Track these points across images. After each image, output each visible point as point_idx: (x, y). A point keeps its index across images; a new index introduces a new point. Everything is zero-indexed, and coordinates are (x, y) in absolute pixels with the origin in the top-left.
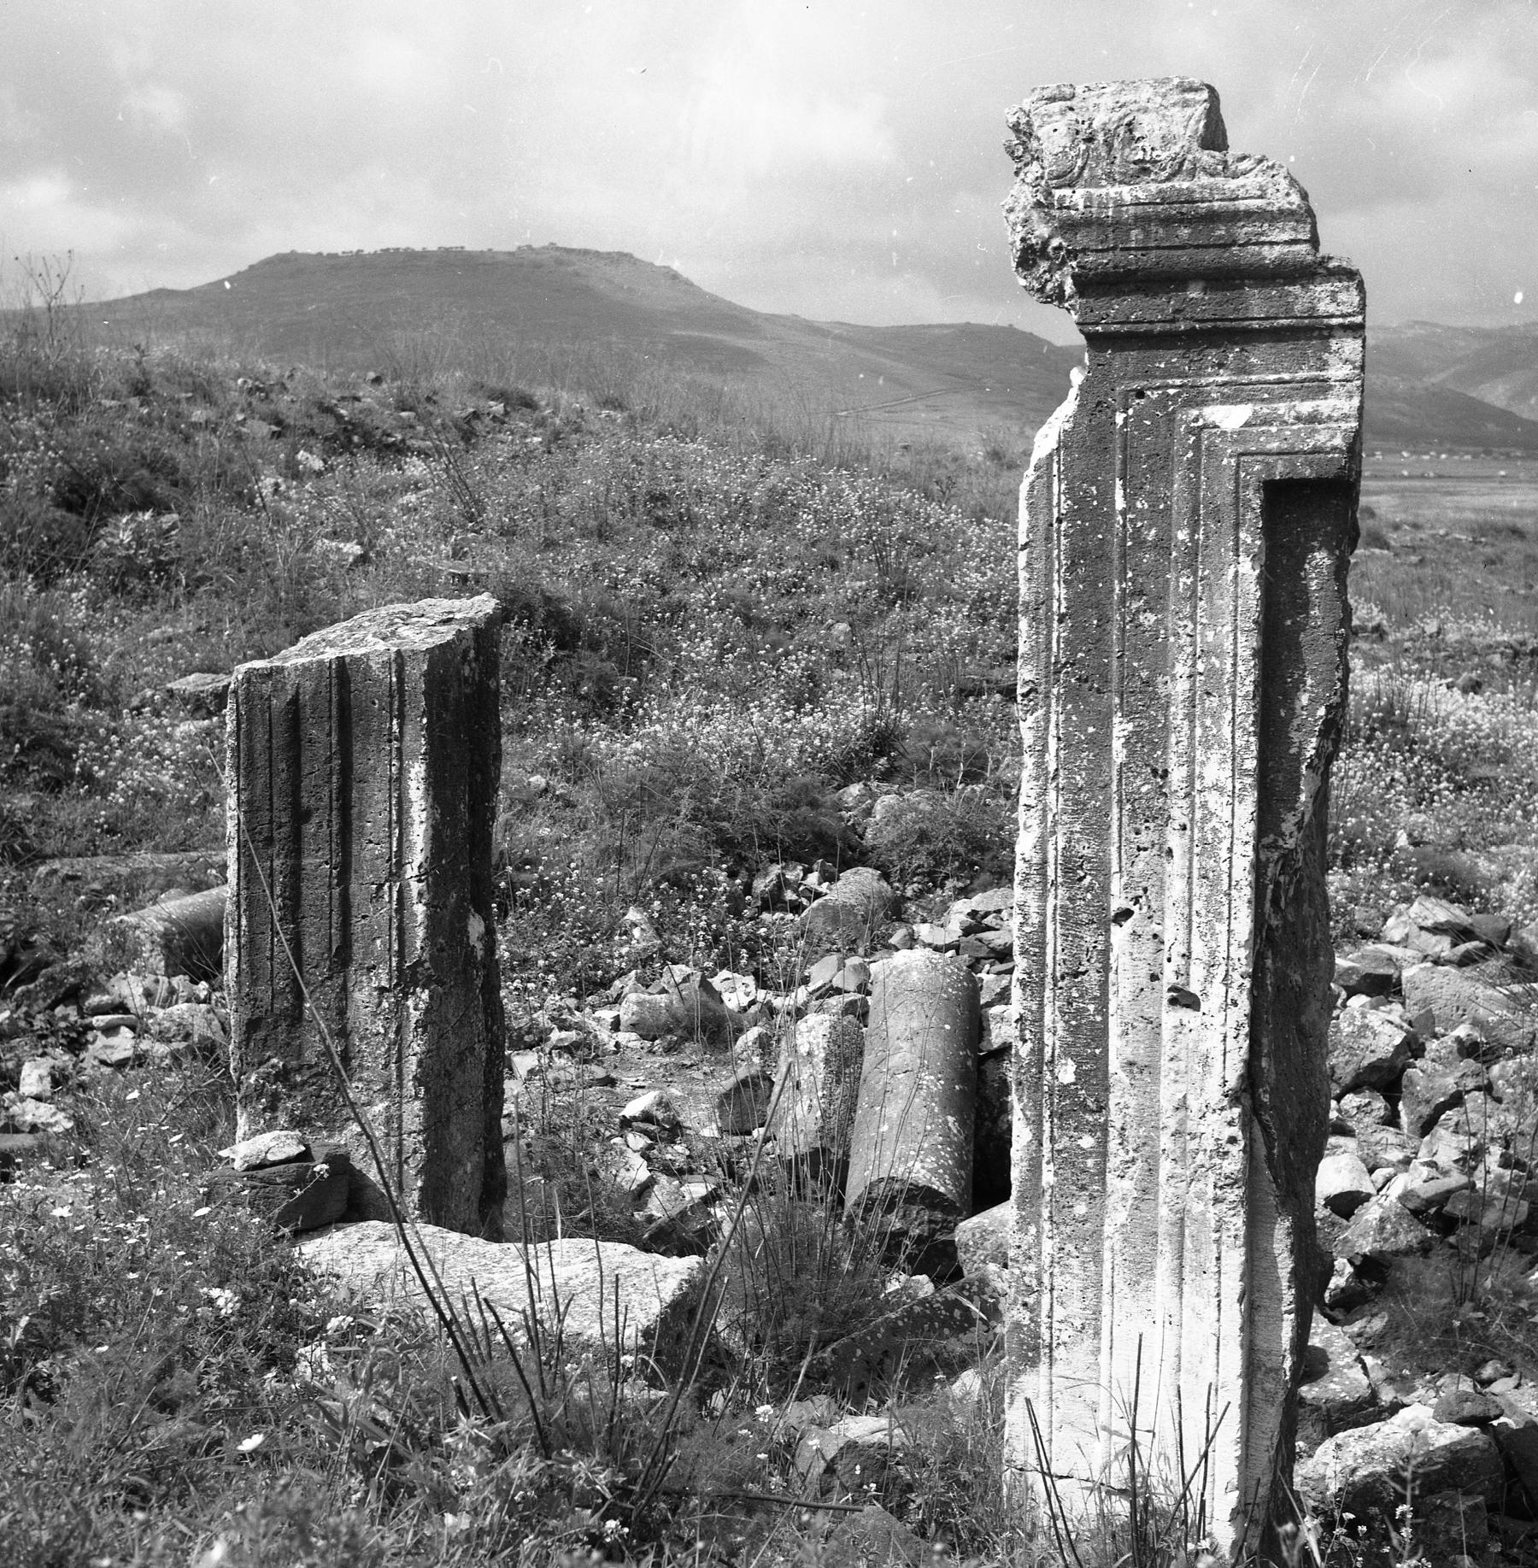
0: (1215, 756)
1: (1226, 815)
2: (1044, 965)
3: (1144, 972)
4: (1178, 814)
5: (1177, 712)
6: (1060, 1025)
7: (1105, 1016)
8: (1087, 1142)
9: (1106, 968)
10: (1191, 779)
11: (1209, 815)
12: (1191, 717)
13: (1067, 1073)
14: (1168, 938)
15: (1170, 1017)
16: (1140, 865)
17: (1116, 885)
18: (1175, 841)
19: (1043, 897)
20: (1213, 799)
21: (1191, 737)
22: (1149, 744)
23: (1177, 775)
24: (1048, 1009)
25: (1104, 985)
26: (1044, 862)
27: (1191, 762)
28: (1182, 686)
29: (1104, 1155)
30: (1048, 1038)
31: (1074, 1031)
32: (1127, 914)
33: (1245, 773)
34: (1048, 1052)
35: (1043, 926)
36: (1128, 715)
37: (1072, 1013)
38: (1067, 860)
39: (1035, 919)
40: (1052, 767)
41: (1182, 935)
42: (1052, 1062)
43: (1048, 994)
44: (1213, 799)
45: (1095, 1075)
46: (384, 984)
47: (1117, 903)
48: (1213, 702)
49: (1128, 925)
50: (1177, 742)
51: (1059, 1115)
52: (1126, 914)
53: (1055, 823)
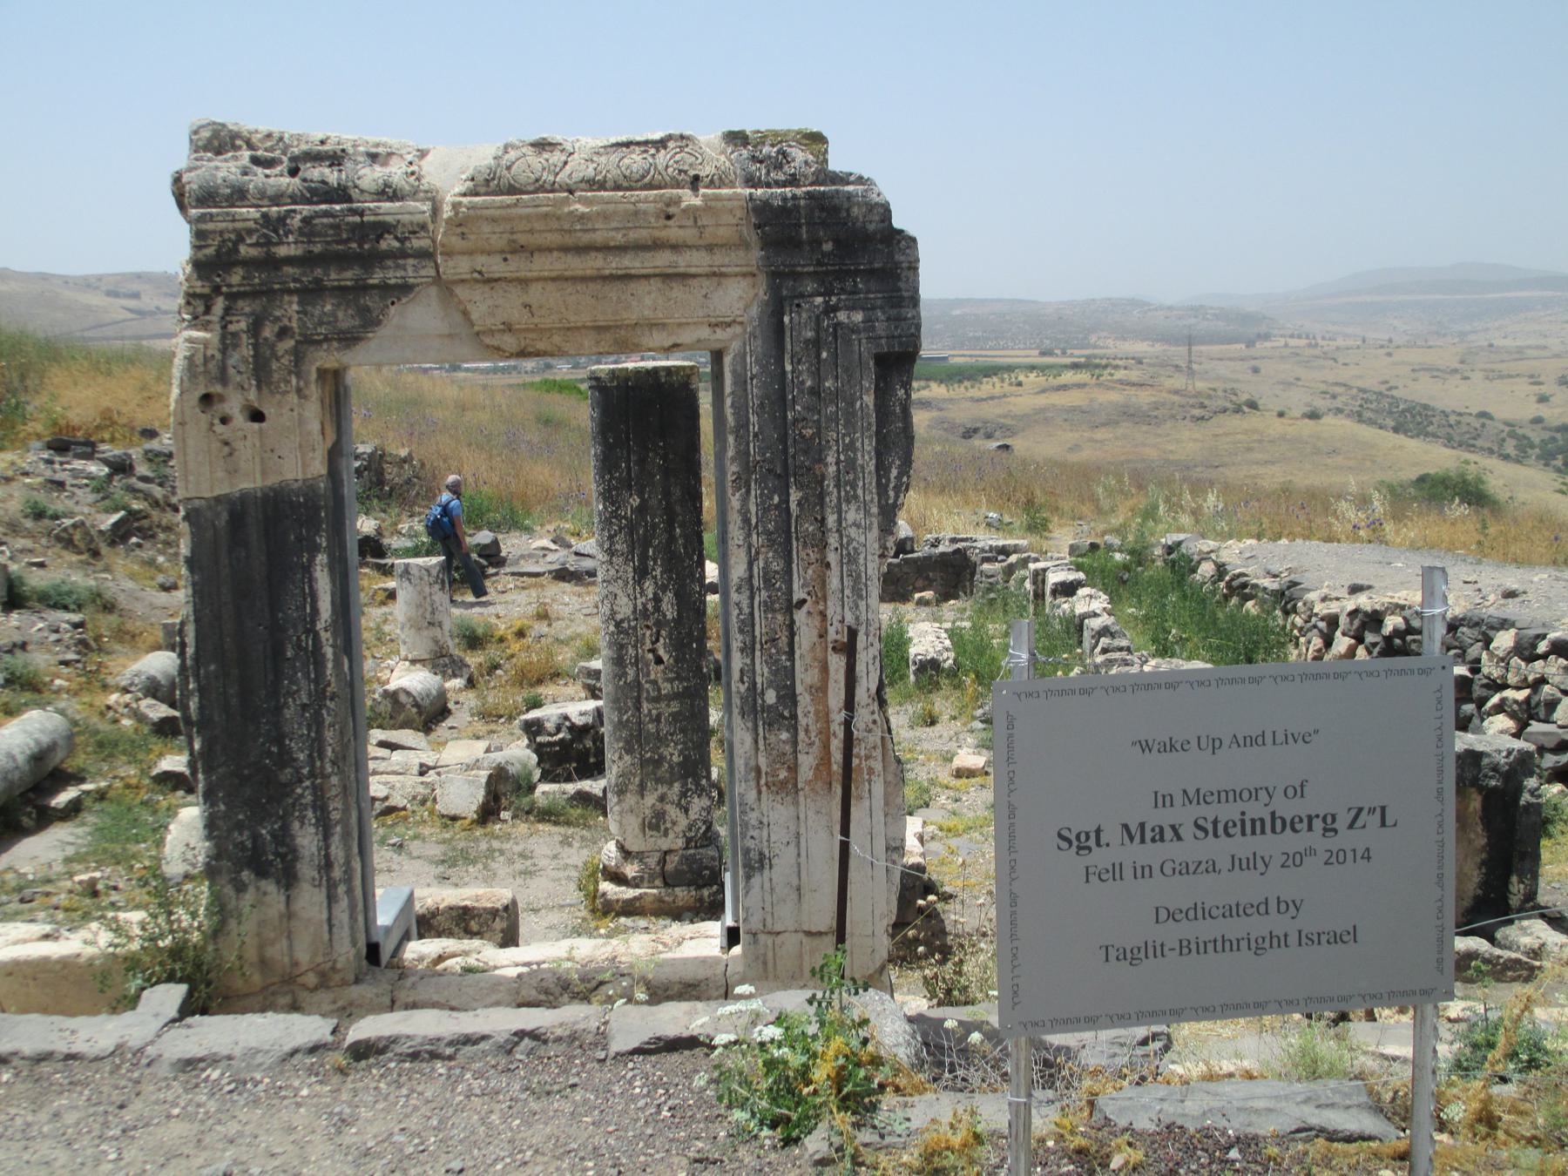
0: (853, 507)
1: (862, 539)
2: (754, 637)
3: (815, 633)
4: (833, 540)
5: (830, 484)
6: (766, 670)
7: (793, 661)
8: (784, 736)
9: (792, 635)
10: (839, 521)
11: (851, 540)
12: (838, 486)
13: (771, 697)
14: (830, 613)
16: (810, 572)
17: (795, 586)
18: (832, 558)
19: (752, 598)
20: (853, 532)
21: (839, 498)
22: (816, 500)
23: (831, 520)
24: (758, 661)
25: (791, 644)
26: (751, 576)
27: (840, 513)
28: (832, 469)
29: (795, 743)
30: (759, 680)
31: (775, 673)
32: (804, 601)
33: (871, 515)
34: (759, 686)
35: (752, 614)
36: (800, 487)
37: (771, 661)
38: (765, 574)
39: (746, 610)
40: (754, 521)
41: (839, 609)
42: (763, 693)
43: (758, 653)
44: (853, 532)
45: (789, 696)
46: (305, 701)
47: (796, 598)
48: (851, 476)
49: (805, 608)
50: (832, 499)
51: (769, 725)
52: (804, 601)
53: (757, 553)
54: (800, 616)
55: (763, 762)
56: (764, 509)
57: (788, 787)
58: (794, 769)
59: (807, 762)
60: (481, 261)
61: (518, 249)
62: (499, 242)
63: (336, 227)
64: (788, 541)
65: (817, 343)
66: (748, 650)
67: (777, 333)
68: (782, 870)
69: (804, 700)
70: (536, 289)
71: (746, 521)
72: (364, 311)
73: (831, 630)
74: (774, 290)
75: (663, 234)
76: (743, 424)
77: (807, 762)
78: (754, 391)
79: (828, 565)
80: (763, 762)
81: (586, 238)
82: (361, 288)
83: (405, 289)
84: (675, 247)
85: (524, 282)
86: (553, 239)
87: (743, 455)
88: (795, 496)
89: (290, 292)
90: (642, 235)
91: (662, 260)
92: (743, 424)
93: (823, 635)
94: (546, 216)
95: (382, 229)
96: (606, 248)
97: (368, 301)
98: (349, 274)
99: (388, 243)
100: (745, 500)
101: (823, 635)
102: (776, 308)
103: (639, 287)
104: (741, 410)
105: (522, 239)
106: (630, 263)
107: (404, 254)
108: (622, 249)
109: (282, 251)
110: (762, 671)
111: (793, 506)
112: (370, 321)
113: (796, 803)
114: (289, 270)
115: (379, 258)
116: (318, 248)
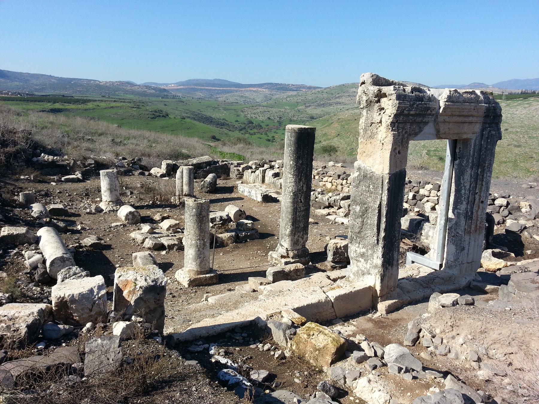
15: (481, 205)
37: (471, 206)
45: (472, 213)
54: (477, 196)
55: (466, 227)
56: (474, 173)
57: (469, 233)
58: (470, 229)
59: (473, 226)
60: (445, 117)
61: (452, 115)
62: (450, 114)
63: (421, 107)
64: (477, 180)
65: (488, 138)
66: (467, 204)
67: (482, 135)
68: (466, 251)
69: (475, 213)
70: (451, 124)
71: (471, 176)
72: (420, 127)
73: (482, 200)
74: (483, 126)
75: (473, 113)
76: (474, 155)
77: (473, 226)
78: (477, 148)
79: (482, 185)
80: (466, 227)
81: (463, 113)
82: (421, 122)
83: (427, 123)
84: (473, 116)
85: (449, 122)
86: (457, 113)
87: (473, 161)
88: (480, 170)
89: (408, 122)
90: (470, 113)
91: (471, 119)
92: (474, 155)
93: (480, 199)
94: (458, 108)
95: (429, 108)
96: (464, 116)
97: (421, 125)
98: (420, 119)
99: (429, 112)
100: (471, 172)
101: (480, 199)
102: (483, 130)
103: (466, 125)
104: (474, 152)
105: (454, 113)
106: (466, 119)
107: (430, 115)
108: (468, 116)
109: (412, 112)
110: (469, 207)
111: (479, 173)
112: (421, 130)
113: (470, 236)
114: (411, 117)
115: (424, 116)
116: (417, 112)
